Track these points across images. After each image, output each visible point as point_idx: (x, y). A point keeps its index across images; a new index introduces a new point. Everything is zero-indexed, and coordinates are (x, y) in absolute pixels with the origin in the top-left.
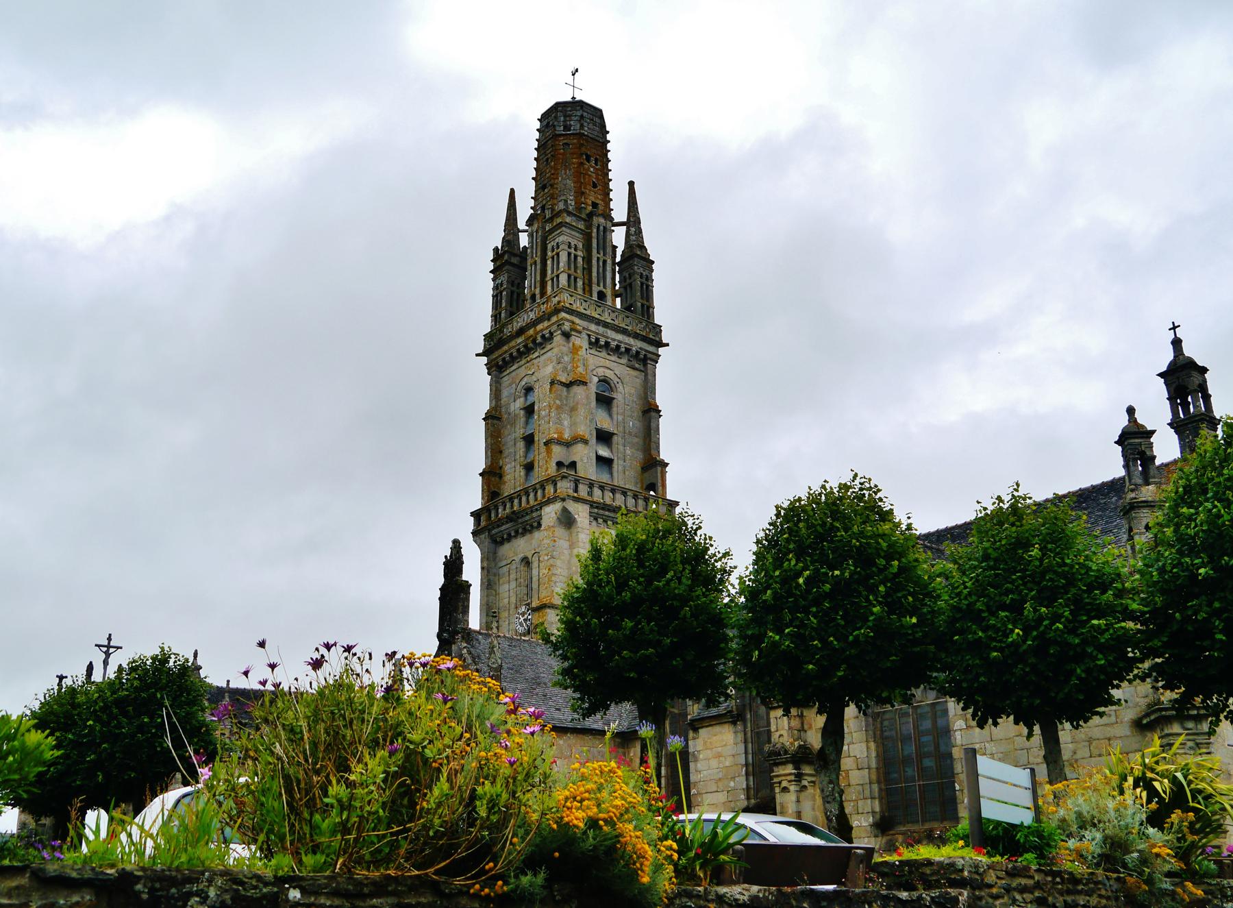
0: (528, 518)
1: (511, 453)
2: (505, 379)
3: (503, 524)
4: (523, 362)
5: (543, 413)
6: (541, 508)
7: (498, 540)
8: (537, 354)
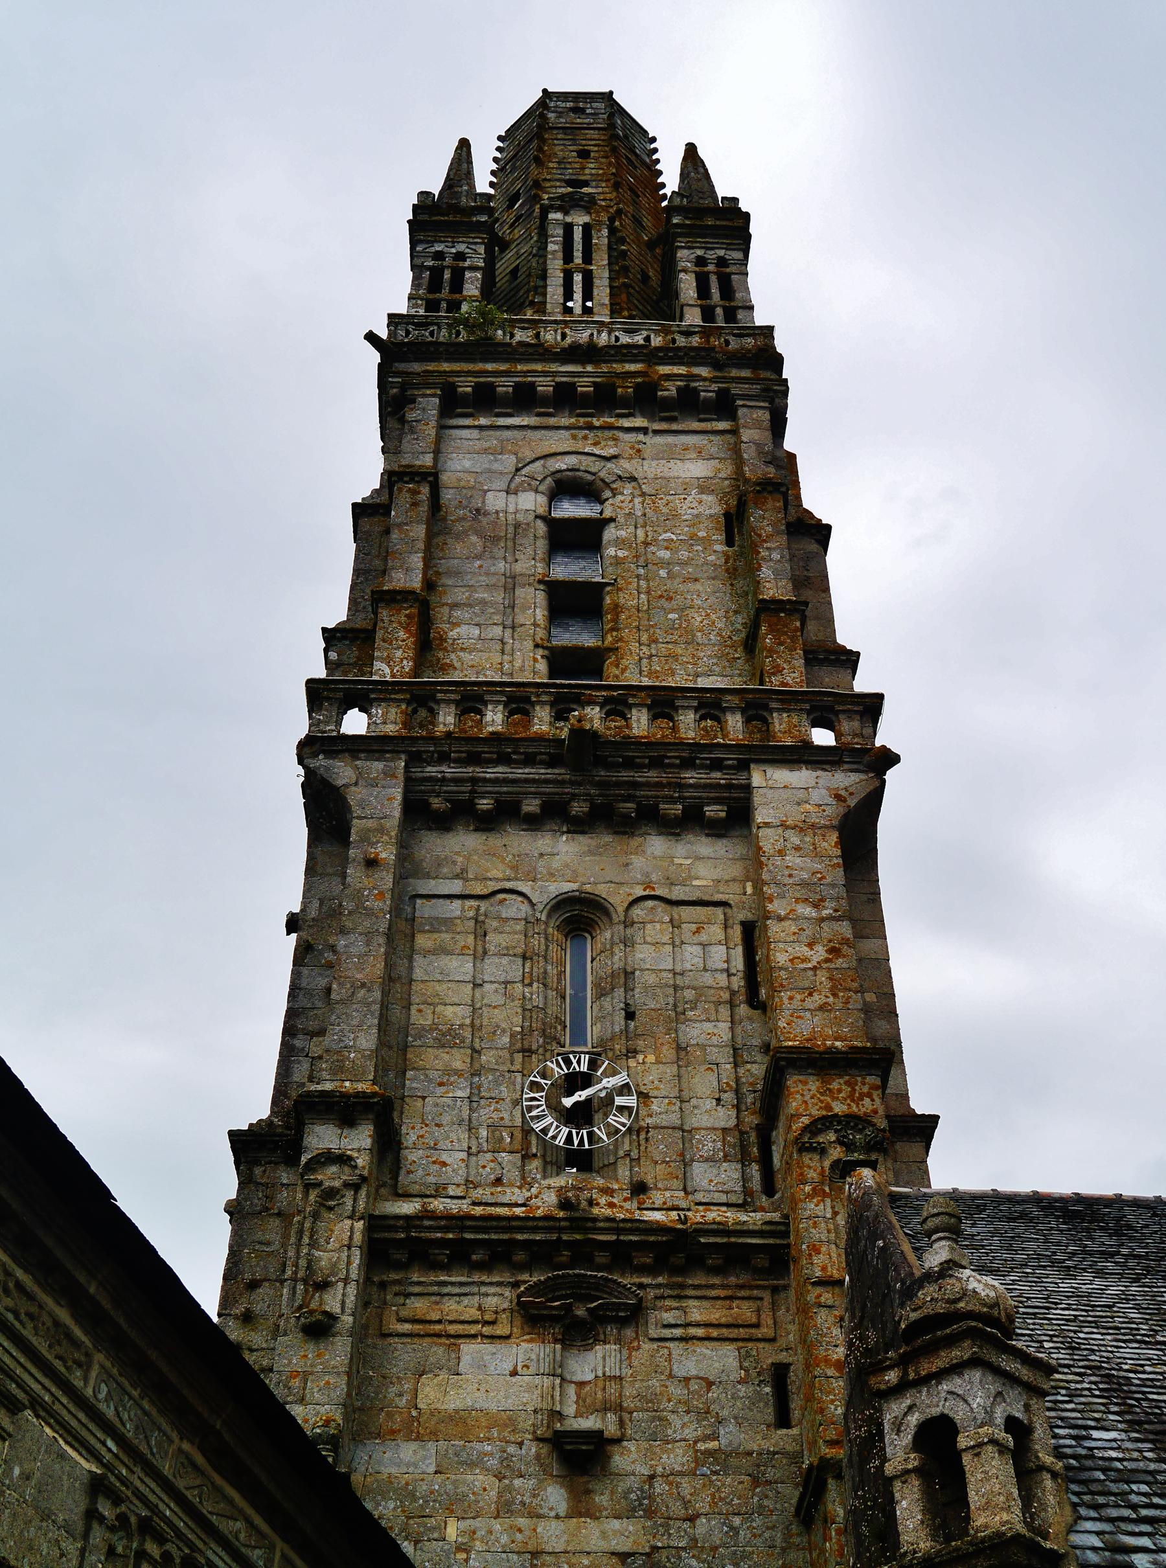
0: (652, 775)
1: (483, 602)
2: (465, 433)
3: (504, 759)
4: (565, 421)
5: (665, 554)
6: (744, 766)
7: (436, 803)
8: (639, 422)
